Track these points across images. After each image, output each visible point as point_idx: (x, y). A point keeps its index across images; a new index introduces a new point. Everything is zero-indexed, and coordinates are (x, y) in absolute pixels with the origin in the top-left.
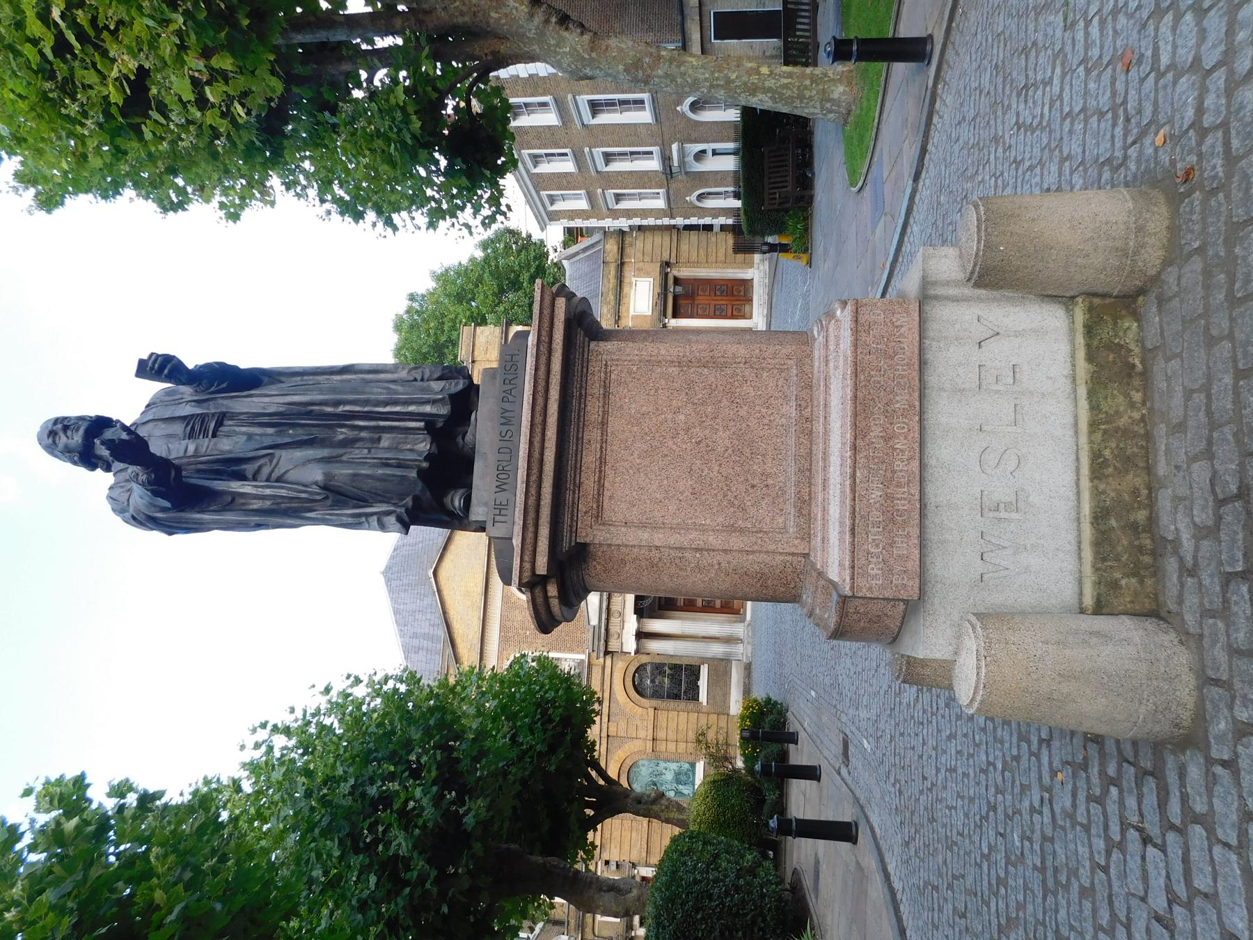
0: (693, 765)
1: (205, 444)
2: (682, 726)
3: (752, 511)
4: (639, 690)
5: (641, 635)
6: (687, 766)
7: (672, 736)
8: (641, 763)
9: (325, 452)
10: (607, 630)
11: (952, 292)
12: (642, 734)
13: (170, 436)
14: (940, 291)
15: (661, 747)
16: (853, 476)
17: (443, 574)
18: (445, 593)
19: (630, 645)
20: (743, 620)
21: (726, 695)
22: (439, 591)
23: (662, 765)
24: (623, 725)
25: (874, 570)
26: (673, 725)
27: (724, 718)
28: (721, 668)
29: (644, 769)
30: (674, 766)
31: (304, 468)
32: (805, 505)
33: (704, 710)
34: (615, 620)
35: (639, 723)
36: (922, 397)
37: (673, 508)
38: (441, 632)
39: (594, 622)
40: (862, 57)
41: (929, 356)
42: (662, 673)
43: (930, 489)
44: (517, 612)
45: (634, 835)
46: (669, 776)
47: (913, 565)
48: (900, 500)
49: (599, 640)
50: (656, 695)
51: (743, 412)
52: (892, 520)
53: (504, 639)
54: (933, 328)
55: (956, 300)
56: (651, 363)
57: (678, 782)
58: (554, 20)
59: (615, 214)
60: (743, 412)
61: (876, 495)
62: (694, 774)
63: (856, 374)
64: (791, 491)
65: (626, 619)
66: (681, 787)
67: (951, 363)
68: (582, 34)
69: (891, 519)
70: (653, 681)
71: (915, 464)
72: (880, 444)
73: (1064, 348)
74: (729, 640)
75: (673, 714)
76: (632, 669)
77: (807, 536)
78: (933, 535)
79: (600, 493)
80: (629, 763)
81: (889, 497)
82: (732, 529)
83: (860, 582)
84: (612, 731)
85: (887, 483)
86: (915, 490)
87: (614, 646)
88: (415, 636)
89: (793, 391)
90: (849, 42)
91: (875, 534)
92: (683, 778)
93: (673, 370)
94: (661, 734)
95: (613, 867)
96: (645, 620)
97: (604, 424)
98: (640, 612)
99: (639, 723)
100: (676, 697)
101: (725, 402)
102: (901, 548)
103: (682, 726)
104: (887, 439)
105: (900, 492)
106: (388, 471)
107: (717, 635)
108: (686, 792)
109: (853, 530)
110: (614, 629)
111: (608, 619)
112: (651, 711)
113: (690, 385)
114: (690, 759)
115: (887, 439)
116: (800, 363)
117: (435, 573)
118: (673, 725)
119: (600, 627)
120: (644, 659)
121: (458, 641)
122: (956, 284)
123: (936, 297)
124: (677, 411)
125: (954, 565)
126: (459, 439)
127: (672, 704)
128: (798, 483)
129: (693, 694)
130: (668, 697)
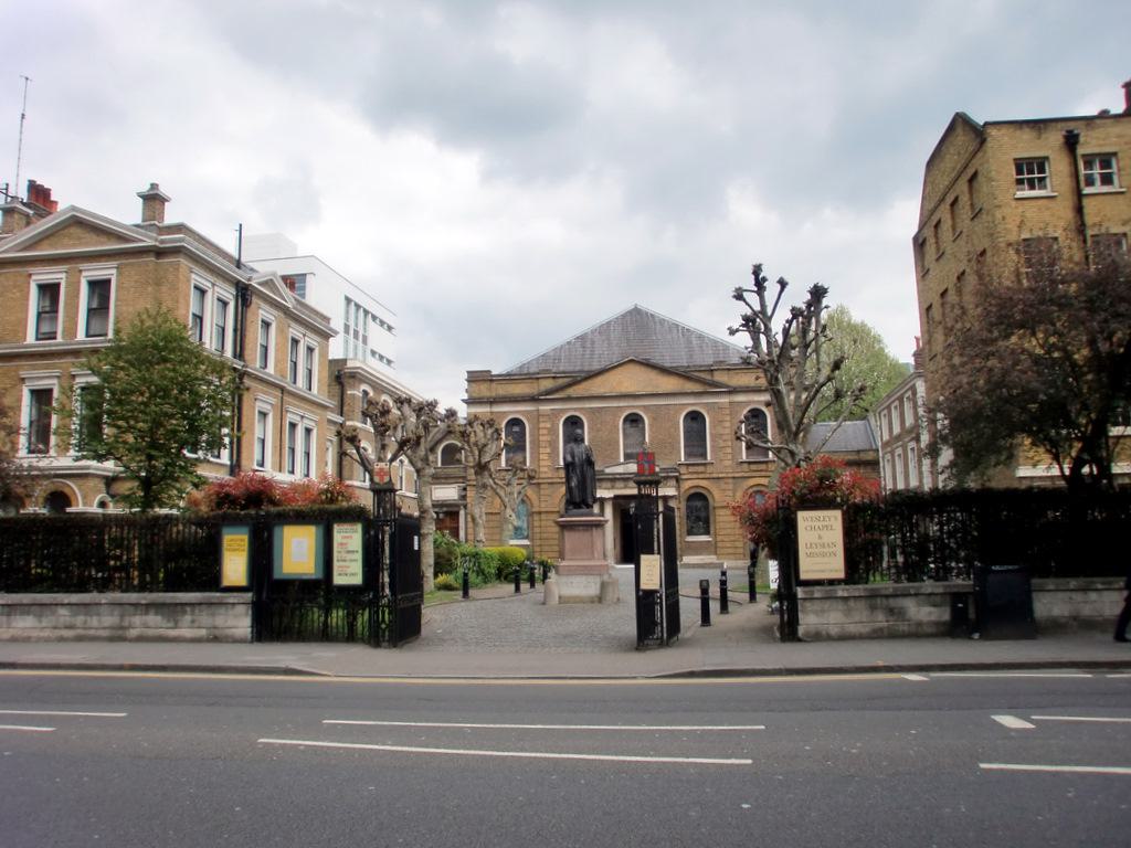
0: (527, 538)
7: (543, 523)
12: (543, 505)
15: (536, 517)
24: (547, 492)
30: (525, 526)
31: (574, 483)
34: (609, 485)
38: (596, 366)
48: (572, 571)
59: (883, 458)
67: (591, 579)
84: (542, 486)
88: (593, 342)
92: (519, 532)
94: (543, 516)
95: (463, 493)
96: (611, 502)
98: (616, 498)
111: (608, 479)
117: (631, 361)
125: (564, 579)
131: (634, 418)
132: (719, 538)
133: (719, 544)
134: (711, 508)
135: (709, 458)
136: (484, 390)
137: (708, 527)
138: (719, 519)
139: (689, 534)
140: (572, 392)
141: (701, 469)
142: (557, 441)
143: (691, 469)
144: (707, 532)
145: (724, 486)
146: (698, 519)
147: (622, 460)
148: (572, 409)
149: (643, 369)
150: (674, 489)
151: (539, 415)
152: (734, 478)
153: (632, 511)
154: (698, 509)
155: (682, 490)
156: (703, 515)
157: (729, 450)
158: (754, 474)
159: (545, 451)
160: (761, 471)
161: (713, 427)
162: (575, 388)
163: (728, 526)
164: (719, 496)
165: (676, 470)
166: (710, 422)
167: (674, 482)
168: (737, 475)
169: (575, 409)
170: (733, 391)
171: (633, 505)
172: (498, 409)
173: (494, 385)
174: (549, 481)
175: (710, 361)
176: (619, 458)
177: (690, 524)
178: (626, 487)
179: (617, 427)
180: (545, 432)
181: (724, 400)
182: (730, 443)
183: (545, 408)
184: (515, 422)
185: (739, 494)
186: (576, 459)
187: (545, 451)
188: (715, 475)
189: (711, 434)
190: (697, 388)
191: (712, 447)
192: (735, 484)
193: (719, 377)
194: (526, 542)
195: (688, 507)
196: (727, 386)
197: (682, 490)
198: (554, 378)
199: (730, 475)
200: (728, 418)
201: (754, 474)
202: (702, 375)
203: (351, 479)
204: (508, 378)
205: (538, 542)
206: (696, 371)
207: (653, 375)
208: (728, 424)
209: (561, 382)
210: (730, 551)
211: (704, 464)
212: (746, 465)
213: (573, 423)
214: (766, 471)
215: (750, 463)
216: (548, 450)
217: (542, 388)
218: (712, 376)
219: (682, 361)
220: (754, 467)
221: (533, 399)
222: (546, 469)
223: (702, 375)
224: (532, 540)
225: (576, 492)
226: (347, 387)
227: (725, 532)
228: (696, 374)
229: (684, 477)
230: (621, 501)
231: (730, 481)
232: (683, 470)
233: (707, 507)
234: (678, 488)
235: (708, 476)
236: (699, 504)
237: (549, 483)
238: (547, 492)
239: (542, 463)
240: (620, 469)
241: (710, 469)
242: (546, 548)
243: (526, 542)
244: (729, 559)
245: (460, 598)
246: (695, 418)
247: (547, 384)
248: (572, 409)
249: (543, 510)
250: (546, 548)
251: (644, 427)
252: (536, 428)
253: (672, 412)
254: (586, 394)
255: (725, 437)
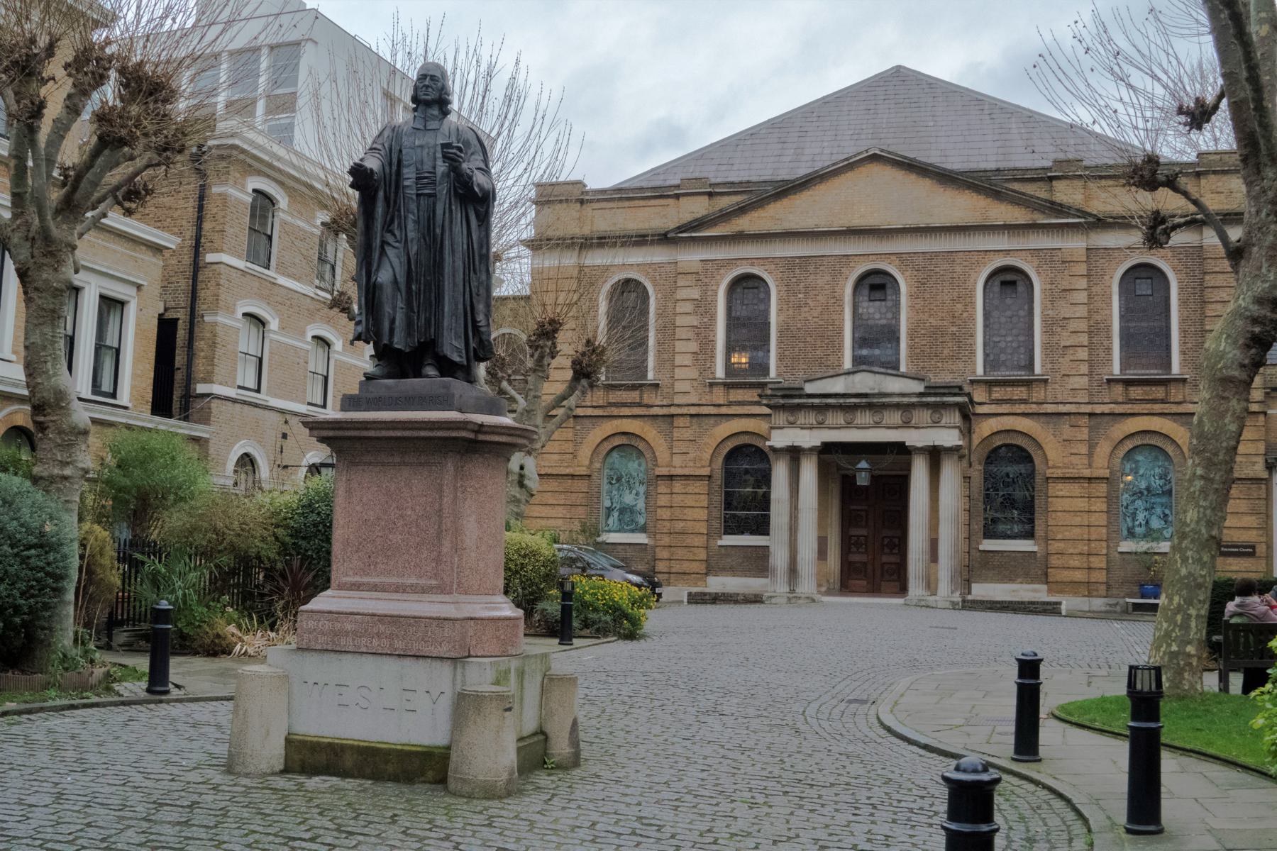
0: (643, 529)
1: (412, 192)
2: (690, 514)
3: (356, 557)
4: (733, 455)
5: (794, 454)
6: (641, 521)
7: (677, 499)
8: (642, 460)
9: (402, 280)
10: (799, 407)
11: (459, 677)
12: (677, 460)
13: (422, 162)
14: (459, 670)
15: (662, 488)
16: (358, 614)
17: (876, 169)
18: (850, 175)
19: (780, 439)
20: (829, 592)
21: (732, 571)
22: (850, 166)
23: (642, 489)
24: (688, 434)
25: (311, 624)
26: (690, 501)
27: (702, 568)
28: (758, 562)
29: (636, 465)
30: (641, 505)
32: (357, 587)
33: (712, 543)
34: (811, 418)
35: (692, 456)
36: (399, 655)
37: (358, 508)
38: (803, 171)
39: (809, 388)
40: (1021, 687)
41: (421, 661)
42: (758, 484)
43: (349, 656)
44: (828, 278)
45: (556, 457)
46: (628, 499)
47: (313, 645)
49: (784, 397)
50: (730, 477)
51: (412, 551)
52: (336, 635)
53: (790, 265)
54: (437, 664)
55: (454, 680)
56: (440, 491)
57: (622, 511)
58: (1257, 329)
60: (412, 551)
61: (348, 626)
62: (632, 531)
63: (415, 617)
64: (365, 579)
65: (815, 432)
66: (616, 514)
67: (416, 672)
68: (1243, 366)
69: (337, 634)
70: (747, 472)
71: (364, 650)
72: (375, 631)
73: (426, 742)
74: (793, 571)
75: (704, 500)
76: (759, 443)
77: (341, 587)
78: (326, 656)
79: (365, 464)
80: (641, 446)
81: (347, 632)
82: (347, 543)
83: (305, 615)
84: (679, 422)
85: (355, 633)
86: (350, 649)
87: (780, 418)
89: (422, 582)
90: (1036, 675)
91: (328, 625)
92: (627, 517)
93: (437, 506)
94: (678, 486)
97: (405, 464)
98: (827, 449)
99: (692, 456)
100: (728, 505)
101: (418, 539)
102: (321, 639)
103: (690, 514)
104: (378, 635)
105: (350, 640)
106: (386, 325)
107: (799, 557)
108: (610, 521)
109: (330, 612)
110: (803, 418)
111: (813, 407)
112: (706, 471)
113: (429, 518)
114: (651, 524)
115: (378, 635)
116: (438, 587)
117: (874, 158)
118: (690, 501)
119: (800, 396)
120: (771, 456)
121: (785, 202)
122: (464, 683)
123: (455, 668)
124: (413, 509)
125: (314, 666)
126: (430, 361)
127: (719, 499)
128: (368, 584)
129: (734, 526)
130: (727, 494)
131: (877, 280)
132: (1055, 547)
133: (1054, 561)
134: (1038, 479)
135: (1038, 369)
136: (569, 222)
137: (1032, 521)
138: (1057, 504)
139: (989, 534)
140: (744, 223)
141: (1019, 393)
142: (709, 327)
143: (998, 393)
144: (1030, 535)
145: (1067, 432)
146: (1009, 502)
147: (848, 364)
148: (746, 258)
149: (899, 175)
150: (956, 432)
151: (676, 273)
152: (1091, 415)
153: (863, 480)
154: (1009, 482)
155: (976, 440)
156: (1019, 494)
157: (1083, 354)
158: (1137, 408)
159: (686, 347)
160: (1154, 401)
161: (1051, 300)
162: (755, 215)
163: (1077, 520)
164: (1057, 451)
165: (959, 390)
166: (1044, 291)
167: (955, 418)
168: (1099, 409)
169: (752, 261)
170: (1100, 223)
171: (863, 464)
172: (597, 259)
173: (588, 209)
174: (693, 410)
175: (1043, 160)
176: (840, 359)
177: (991, 514)
178: (849, 425)
179: (839, 302)
180: (688, 307)
181: (1075, 244)
182: (1084, 339)
183: (690, 257)
184: (628, 286)
185: (1104, 449)
186: (409, 174)
187: (686, 347)
188: (1050, 408)
189: (1045, 321)
190: (1018, 215)
191: (1047, 347)
192: (1091, 429)
193: (1066, 193)
194: (641, 538)
195: (988, 476)
196: (1083, 213)
197: (976, 440)
198: (710, 195)
199: (1088, 409)
200: (1083, 283)
201: (1137, 408)
202: (1029, 189)
203: (208, 380)
204: (624, 195)
205: (666, 540)
206: (1016, 180)
207: (922, 188)
208: (1082, 297)
209: (724, 202)
210: (1079, 576)
211: (1028, 383)
212: (1119, 389)
213: (746, 284)
214: (1163, 401)
215: (1128, 383)
216: (693, 346)
217: (687, 217)
218: (1051, 190)
219: (986, 158)
220: (1136, 392)
221: (665, 239)
222: (685, 386)
223: (1029, 189)
224: (653, 535)
225: (394, 309)
226: (212, 179)
227: (1068, 535)
228: (1016, 186)
229: (980, 410)
230: (842, 460)
231: (1086, 420)
232: (979, 395)
233: (1032, 475)
234: (967, 432)
235: (1034, 408)
236: (1013, 470)
237: (692, 416)
238: (688, 434)
239: (679, 373)
240: (838, 386)
241: (1038, 393)
242: (680, 553)
243: (641, 538)
244: (1076, 594)
245: (138, 688)
246: (1009, 280)
247: (697, 208)
248: (746, 258)
249: (679, 472)
250: (680, 553)
251: (897, 304)
252: (669, 299)
253: (958, 269)
254: (777, 228)
255: (1073, 325)
